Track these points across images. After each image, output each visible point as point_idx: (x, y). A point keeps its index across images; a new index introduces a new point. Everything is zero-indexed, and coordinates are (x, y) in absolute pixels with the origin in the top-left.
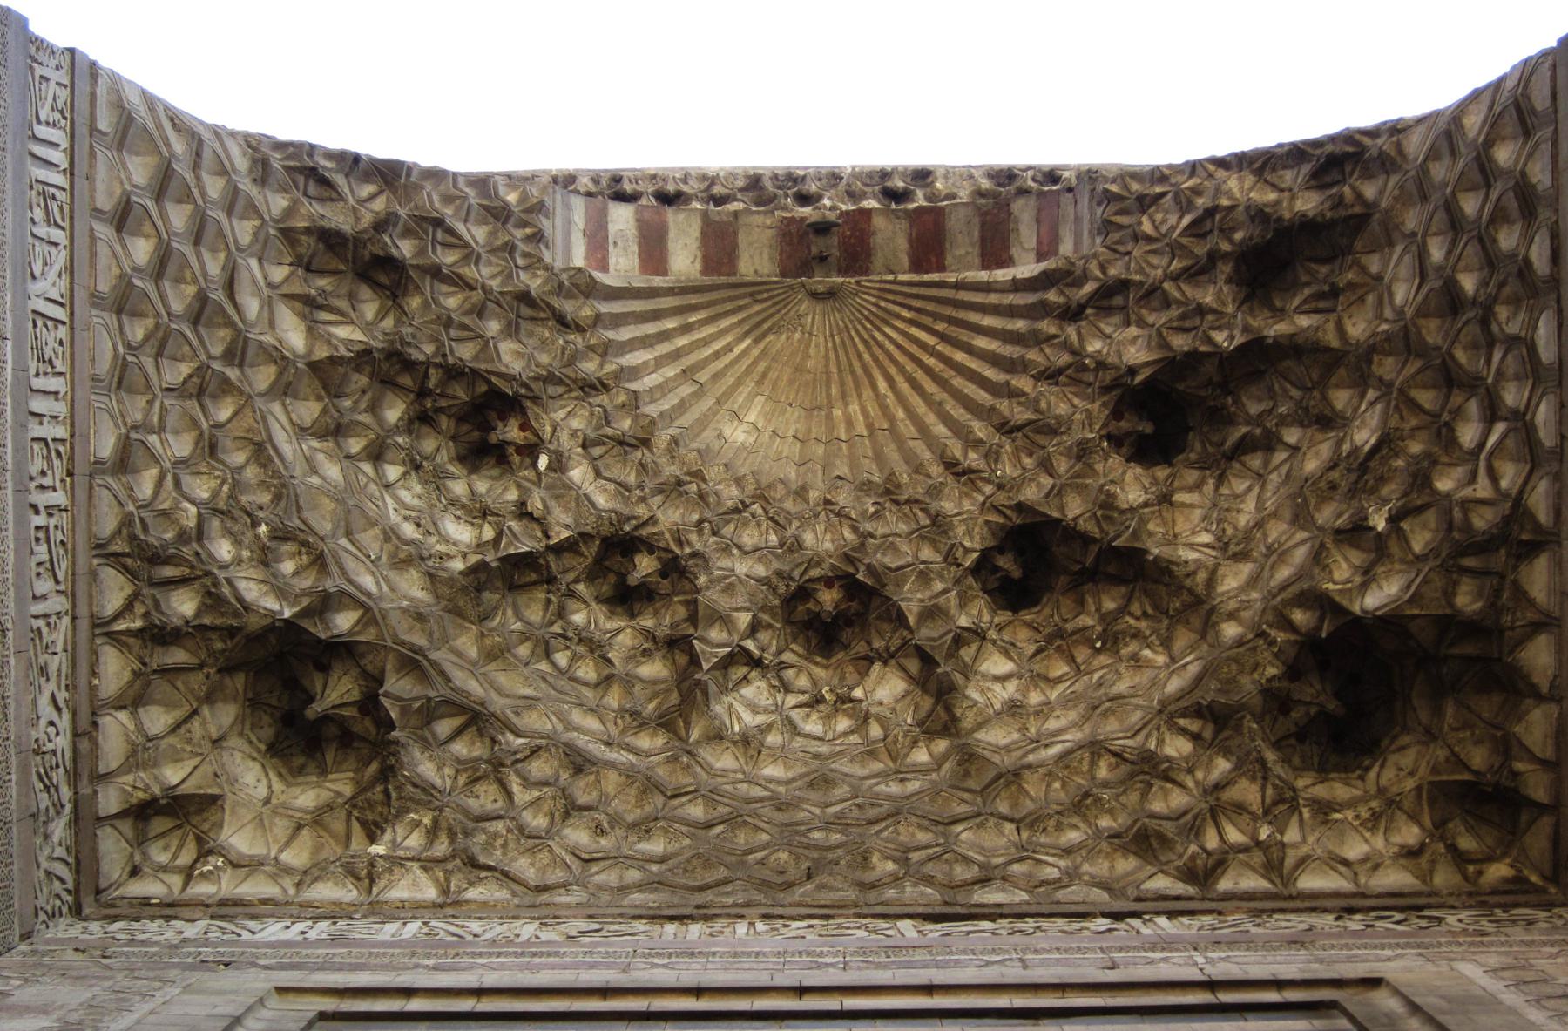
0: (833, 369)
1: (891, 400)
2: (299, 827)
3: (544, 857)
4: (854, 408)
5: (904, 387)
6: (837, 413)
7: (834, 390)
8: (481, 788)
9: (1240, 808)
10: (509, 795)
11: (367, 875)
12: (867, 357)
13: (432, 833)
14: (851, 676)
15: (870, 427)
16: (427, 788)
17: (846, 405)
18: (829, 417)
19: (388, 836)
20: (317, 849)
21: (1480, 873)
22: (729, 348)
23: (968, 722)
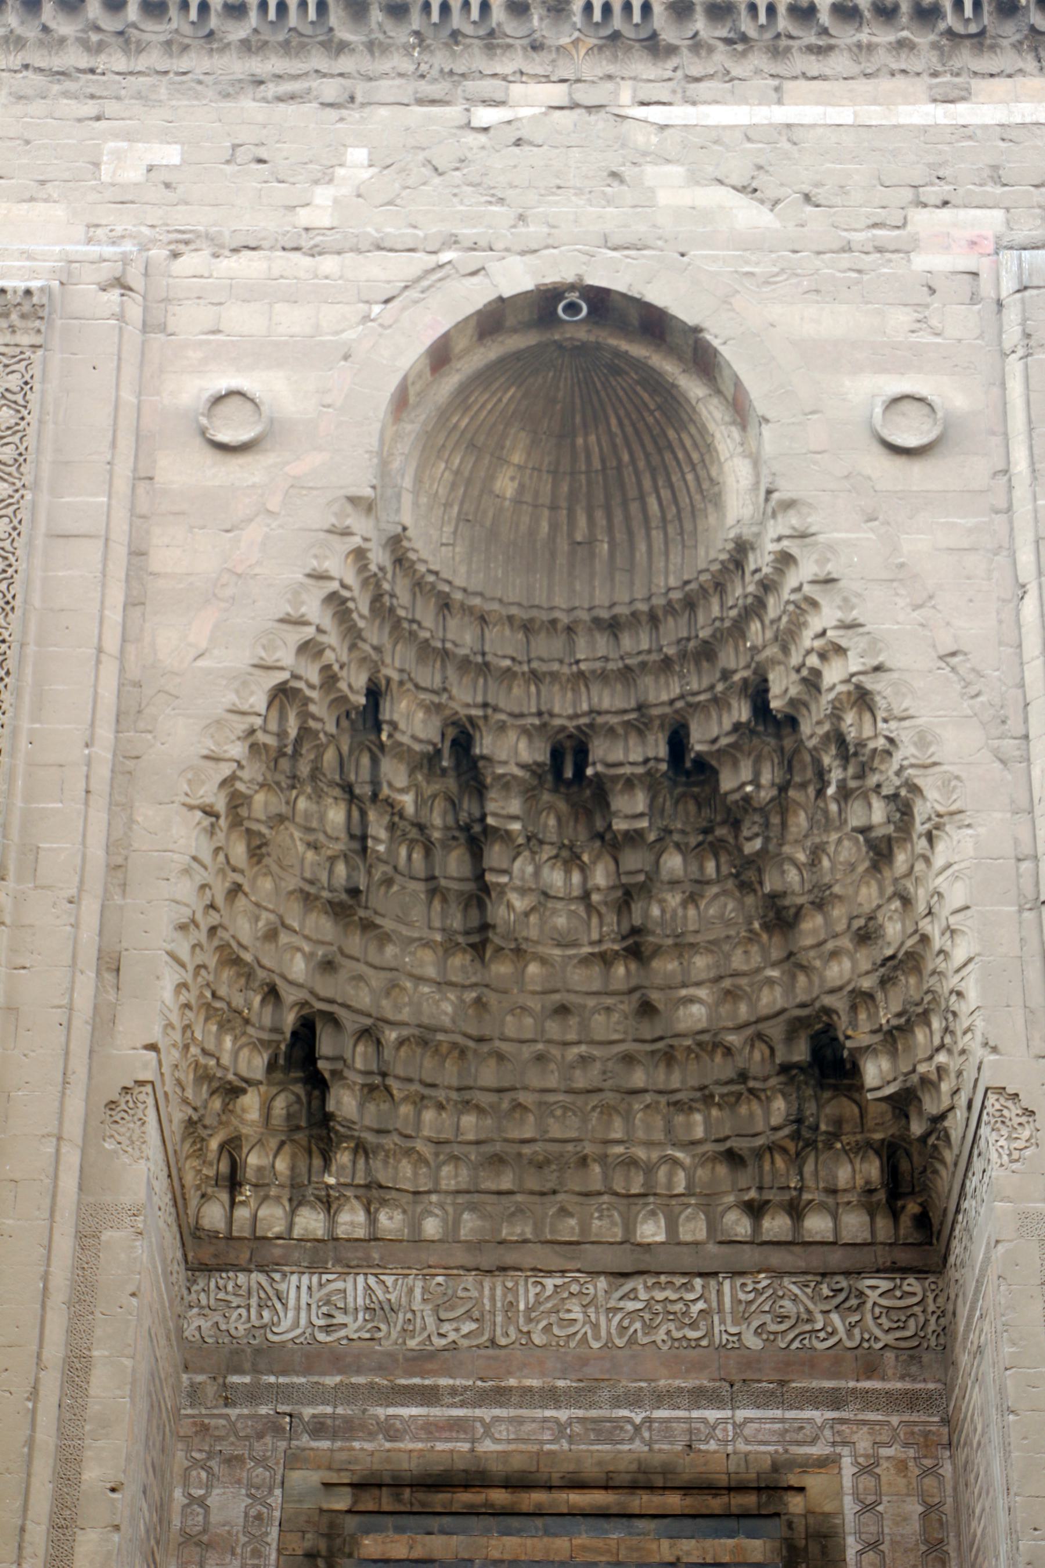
0: (578, 401)
1: (619, 441)
2: (282, 1144)
3: (415, 1156)
4: (592, 438)
5: (629, 430)
6: (580, 441)
7: (578, 419)
8: (375, 1094)
9: (784, 1150)
10: (392, 1095)
11: (328, 1204)
12: (603, 394)
13: (355, 1152)
14: (583, 835)
15: (603, 461)
16: (349, 1124)
17: (586, 435)
18: (573, 445)
19: (334, 1168)
20: (294, 1156)
21: (903, 1207)
22: (500, 400)
23: (647, 951)
